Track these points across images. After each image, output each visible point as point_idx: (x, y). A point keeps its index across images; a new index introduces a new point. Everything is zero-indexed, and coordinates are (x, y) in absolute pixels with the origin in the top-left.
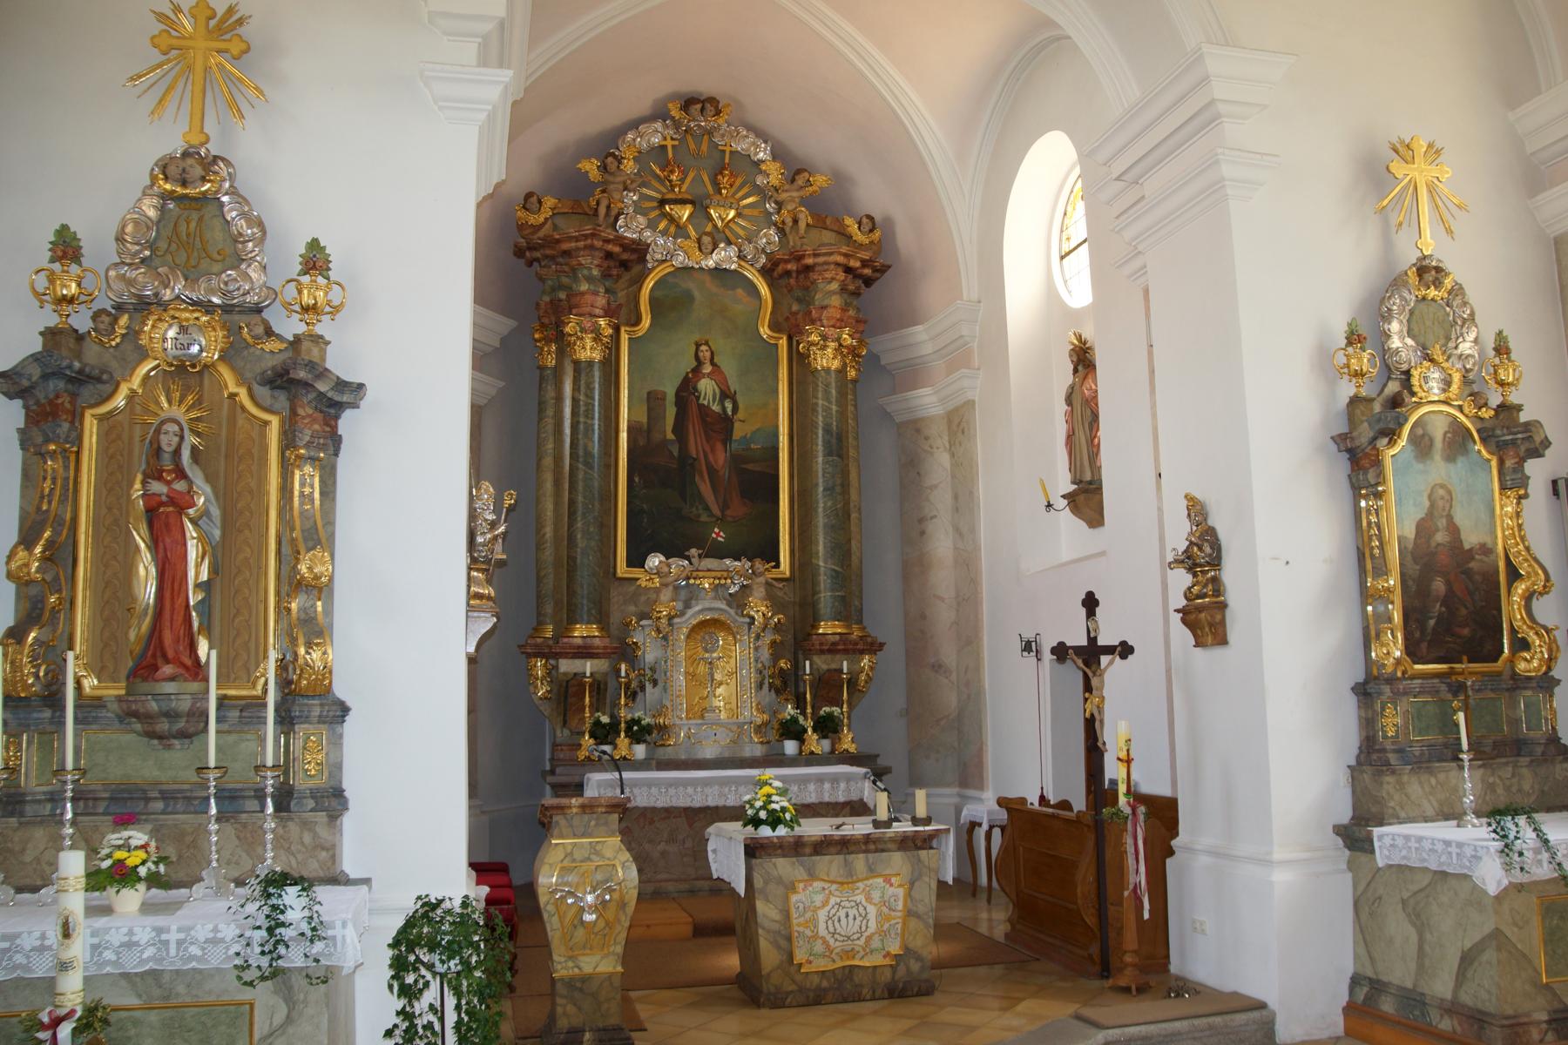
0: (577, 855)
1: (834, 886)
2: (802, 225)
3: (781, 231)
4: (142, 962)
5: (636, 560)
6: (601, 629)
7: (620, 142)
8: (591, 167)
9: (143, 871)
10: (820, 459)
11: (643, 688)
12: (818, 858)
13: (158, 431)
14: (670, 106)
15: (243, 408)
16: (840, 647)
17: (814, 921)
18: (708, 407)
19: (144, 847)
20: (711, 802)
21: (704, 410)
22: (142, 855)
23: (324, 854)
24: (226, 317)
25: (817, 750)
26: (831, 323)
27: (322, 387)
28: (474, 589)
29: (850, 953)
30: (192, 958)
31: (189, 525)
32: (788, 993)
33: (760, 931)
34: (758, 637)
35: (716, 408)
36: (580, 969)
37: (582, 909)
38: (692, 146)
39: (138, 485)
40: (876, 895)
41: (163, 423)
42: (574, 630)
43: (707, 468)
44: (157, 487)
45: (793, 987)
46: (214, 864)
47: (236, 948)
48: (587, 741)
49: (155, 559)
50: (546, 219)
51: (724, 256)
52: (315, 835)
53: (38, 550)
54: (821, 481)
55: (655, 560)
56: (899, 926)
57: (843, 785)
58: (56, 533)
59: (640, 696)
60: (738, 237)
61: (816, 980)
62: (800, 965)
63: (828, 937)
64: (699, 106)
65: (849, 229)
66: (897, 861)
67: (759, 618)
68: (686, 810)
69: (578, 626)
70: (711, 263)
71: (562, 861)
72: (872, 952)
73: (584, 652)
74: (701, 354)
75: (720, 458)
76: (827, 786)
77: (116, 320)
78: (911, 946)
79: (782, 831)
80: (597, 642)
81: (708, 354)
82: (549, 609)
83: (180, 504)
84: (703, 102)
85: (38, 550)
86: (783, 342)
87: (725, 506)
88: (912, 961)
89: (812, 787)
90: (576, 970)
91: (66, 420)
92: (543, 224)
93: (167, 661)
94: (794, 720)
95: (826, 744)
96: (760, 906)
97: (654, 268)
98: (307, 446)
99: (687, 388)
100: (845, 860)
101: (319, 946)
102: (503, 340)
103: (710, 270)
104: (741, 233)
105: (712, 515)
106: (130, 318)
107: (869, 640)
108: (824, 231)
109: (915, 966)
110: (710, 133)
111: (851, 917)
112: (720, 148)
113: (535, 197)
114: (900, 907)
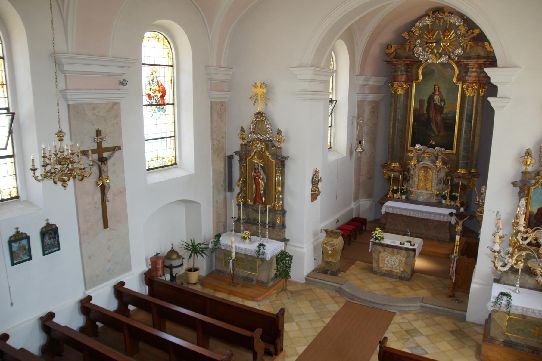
0: (329, 241)
1: (389, 254)
2: (468, 48)
3: (464, 49)
4: (243, 252)
5: (413, 145)
6: (399, 165)
7: (415, 25)
8: (405, 35)
9: (248, 238)
10: (464, 123)
11: (409, 180)
12: (386, 248)
13: (255, 165)
14: (429, 13)
15: (270, 159)
16: (461, 177)
17: (384, 260)
18: (436, 104)
19: (248, 234)
20: (411, 215)
21: (435, 105)
22: (248, 235)
23: (279, 236)
24: (266, 142)
25: (449, 204)
26: (471, 82)
27: (279, 158)
28: (312, 190)
29: (392, 268)
30: (249, 253)
31: (260, 181)
32: (378, 272)
33: (373, 259)
34: (438, 172)
35: (439, 104)
36: (329, 260)
37: (328, 251)
38: (438, 23)
39: (253, 173)
40: (399, 258)
41: (255, 164)
42: (392, 164)
43: (435, 122)
44: (255, 174)
45: (379, 271)
46: (260, 237)
47: (254, 254)
48: (390, 194)
49: (255, 186)
50: (393, 51)
51: (444, 59)
52: (278, 233)
53: (240, 182)
54: (464, 129)
55: (418, 146)
56: (403, 266)
57: (446, 217)
58: (243, 179)
59: (409, 181)
60: (450, 52)
61: (384, 271)
62: (381, 268)
63: (387, 264)
64: (437, 13)
65: (486, 46)
66: (404, 252)
67: (438, 167)
68: (406, 216)
69: (393, 164)
70: (439, 61)
71: (326, 241)
72: (397, 269)
73: (393, 171)
74: (436, 88)
75: (439, 119)
76: (442, 217)
77: (250, 142)
78: (406, 270)
79: (377, 241)
80: (397, 168)
81: (438, 88)
82: (390, 156)
83: (259, 177)
84: (438, 11)
85: (240, 182)
86: (460, 85)
87: (439, 132)
88: (406, 274)
89: (438, 216)
90: (328, 260)
91: (244, 160)
92: (393, 52)
93: (257, 202)
94: (445, 195)
95: (453, 203)
96: (373, 254)
97: (423, 63)
98: (278, 168)
99: (431, 98)
100: (392, 250)
101: (264, 256)
102: (385, 83)
103: (439, 63)
104: (451, 50)
105: (435, 134)
106: (253, 142)
107: (476, 174)
108: (479, 47)
109: (406, 275)
110: (443, 18)
111: (393, 261)
112: (446, 23)
113: (389, 46)
114: (404, 261)
